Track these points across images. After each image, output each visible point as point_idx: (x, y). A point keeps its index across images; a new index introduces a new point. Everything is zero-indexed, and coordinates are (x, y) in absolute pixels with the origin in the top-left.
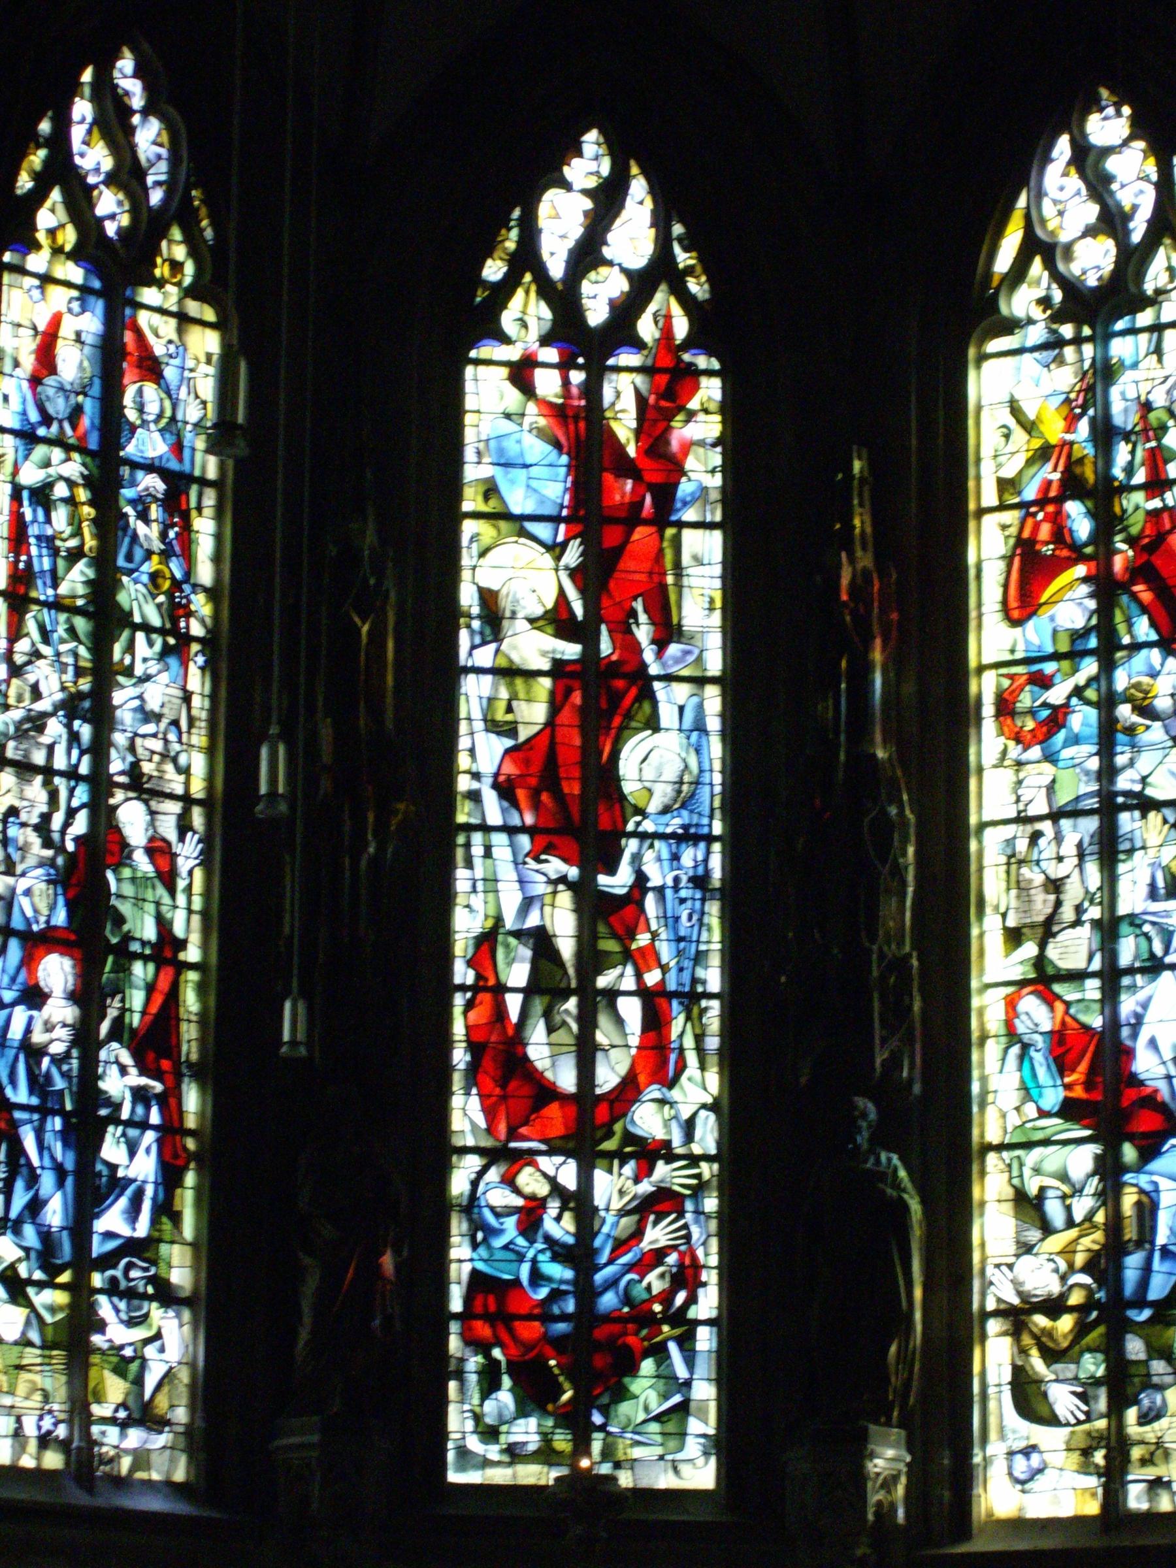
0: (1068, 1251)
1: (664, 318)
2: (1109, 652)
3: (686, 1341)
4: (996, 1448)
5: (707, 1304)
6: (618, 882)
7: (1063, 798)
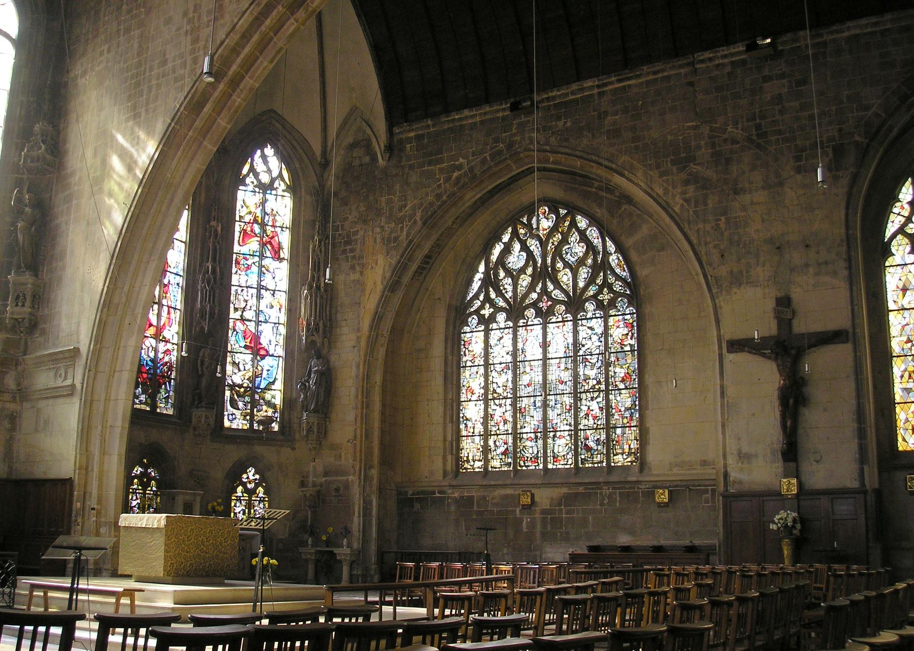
2: (262, 256)
4: (226, 413)
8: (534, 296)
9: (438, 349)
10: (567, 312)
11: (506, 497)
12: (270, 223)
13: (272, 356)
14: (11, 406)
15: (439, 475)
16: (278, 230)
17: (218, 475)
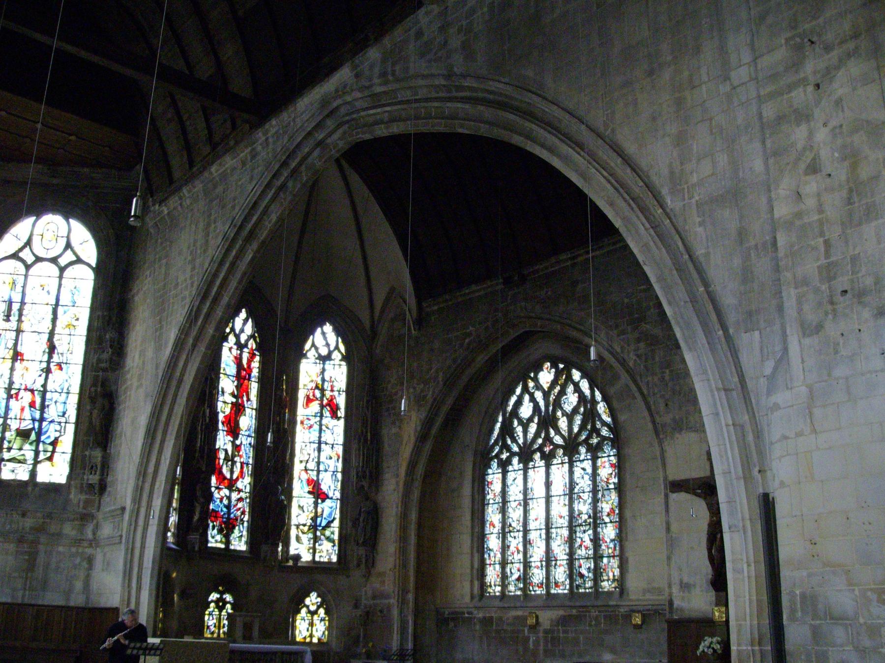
1: (252, 344)
2: (322, 416)
5: (246, 518)
6: (238, 442)
7: (311, 440)
8: (540, 441)
9: (467, 490)
10: (564, 455)
11: (517, 618)
12: (329, 389)
13: (331, 498)
14: (89, 551)
15: (467, 599)
16: (336, 393)
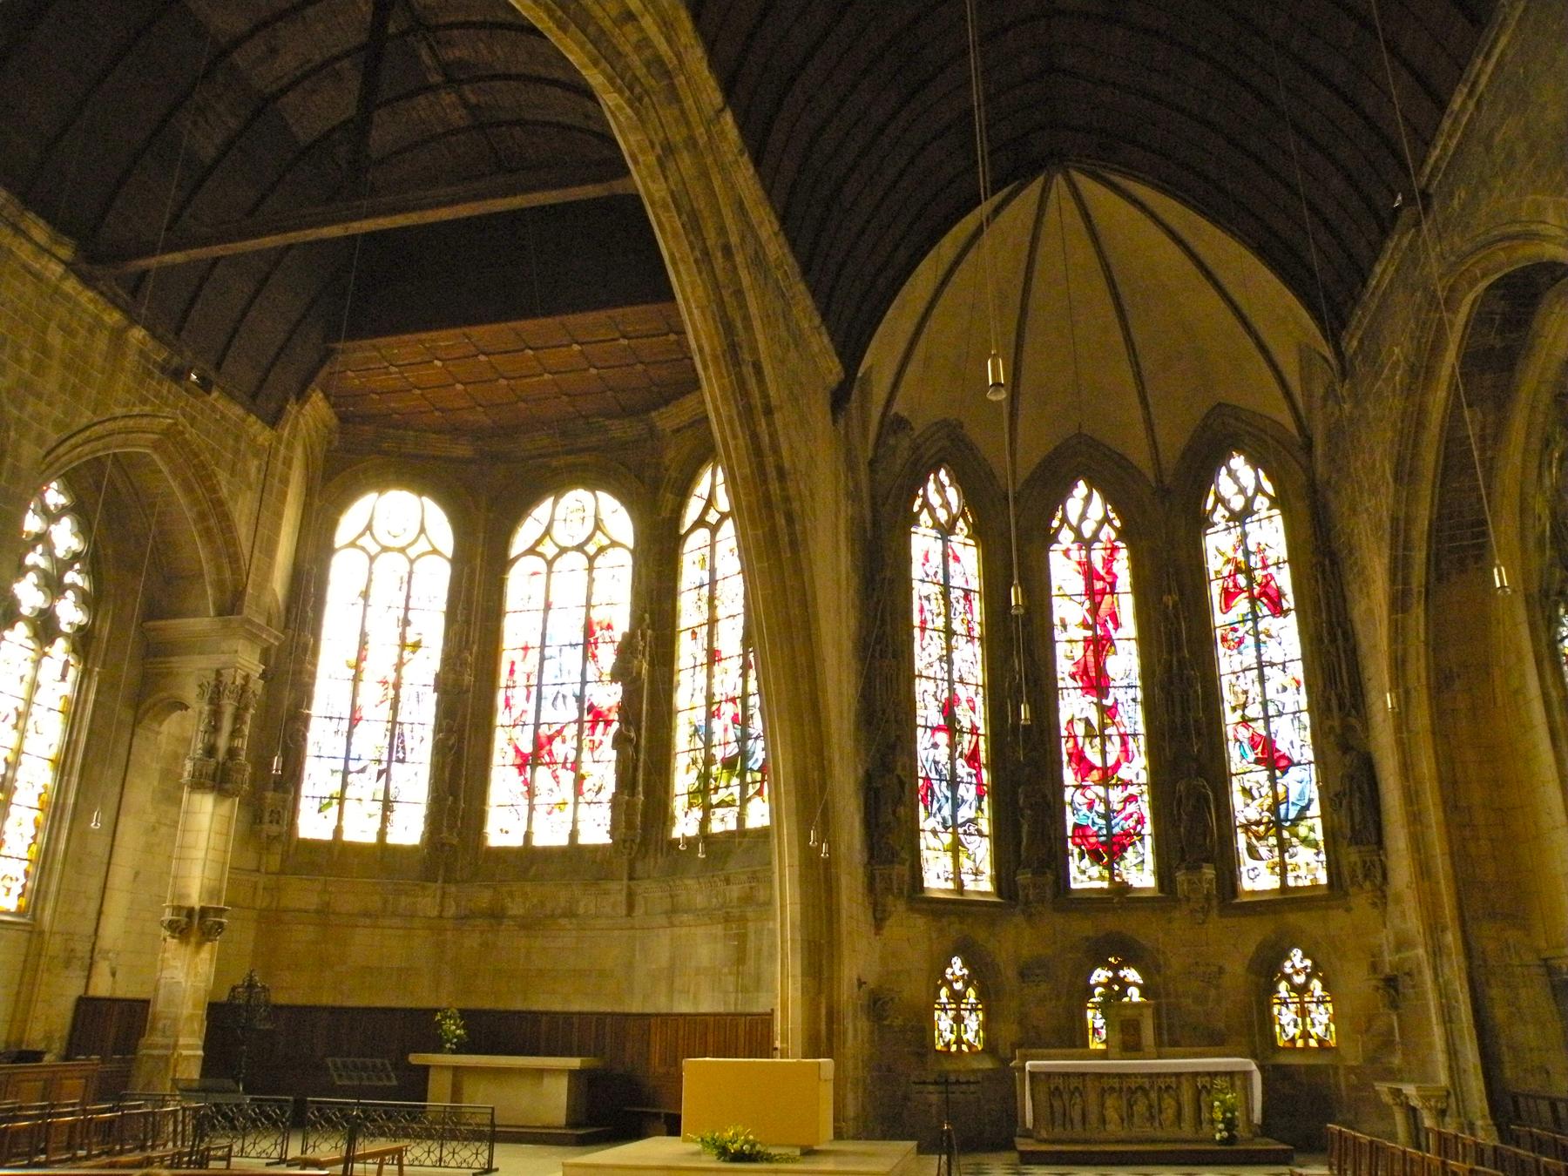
0: (1261, 805)
1: (1108, 532)
3: (1142, 840)
4: (1243, 869)
5: (1148, 829)
6: (1108, 702)
12: (1260, 565)
13: (1299, 764)
17: (1236, 969)
